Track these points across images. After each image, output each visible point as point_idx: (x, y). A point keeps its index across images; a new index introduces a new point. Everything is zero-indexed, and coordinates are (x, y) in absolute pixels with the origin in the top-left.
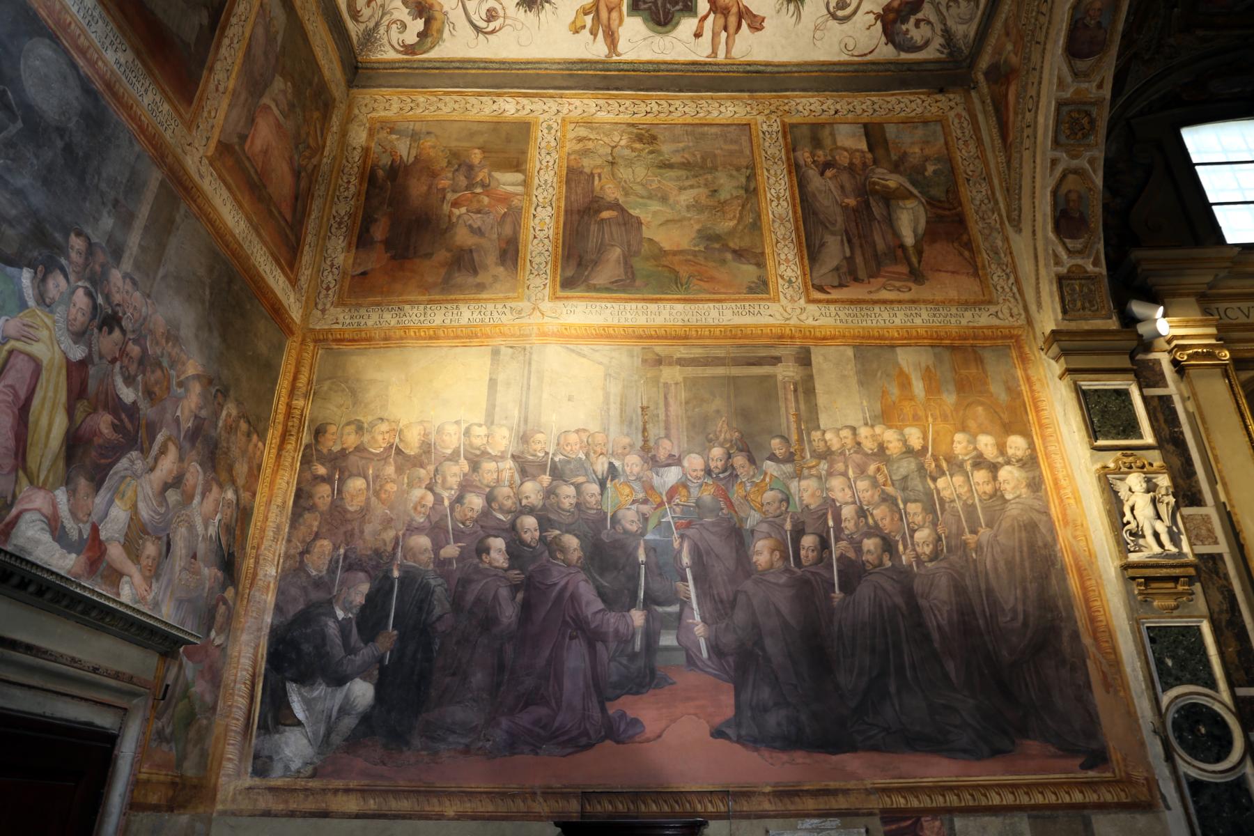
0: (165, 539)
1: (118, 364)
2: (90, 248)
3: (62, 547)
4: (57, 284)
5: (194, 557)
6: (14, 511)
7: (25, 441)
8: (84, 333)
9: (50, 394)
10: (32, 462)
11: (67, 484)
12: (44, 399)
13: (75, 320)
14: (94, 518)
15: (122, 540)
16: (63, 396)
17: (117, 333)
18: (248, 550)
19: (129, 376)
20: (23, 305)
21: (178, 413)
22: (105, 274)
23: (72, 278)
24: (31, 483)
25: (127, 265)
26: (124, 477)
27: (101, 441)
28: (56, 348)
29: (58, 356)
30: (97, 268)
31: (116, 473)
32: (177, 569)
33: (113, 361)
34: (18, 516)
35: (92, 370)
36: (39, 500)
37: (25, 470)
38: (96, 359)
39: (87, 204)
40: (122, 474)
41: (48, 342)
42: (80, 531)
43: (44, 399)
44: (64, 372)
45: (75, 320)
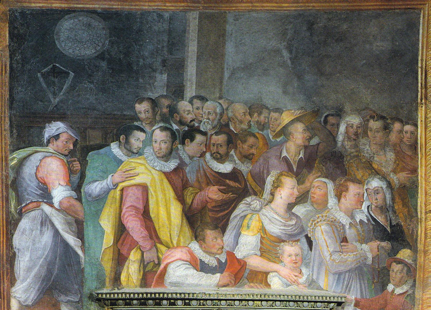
0: (304, 240)
1: (208, 155)
2: (154, 103)
3: (206, 273)
4: (137, 138)
5: (345, 240)
6: (162, 266)
7: (154, 228)
8: (171, 153)
9: (160, 196)
10: (164, 235)
11: (196, 238)
12: (157, 201)
13: (161, 149)
14: (227, 248)
15: (259, 253)
16: (171, 194)
17: (199, 138)
18: (421, 214)
19: (221, 157)
20: (120, 162)
21: (284, 154)
22: (173, 110)
23: (147, 128)
24: (168, 247)
25: (190, 91)
26: (245, 216)
27: (214, 204)
28: (153, 171)
29: (157, 175)
30: (165, 110)
31: (236, 217)
32: (327, 254)
33: (203, 155)
34: (165, 268)
35: (187, 169)
36: (178, 254)
37: (161, 243)
38: (187, 160)
39: (141, 80)
40: (242, 214)
41: (146, 171)
42: (218, 260)
43: (157, 201)
44: (165, 180)
45: (161, 149)
